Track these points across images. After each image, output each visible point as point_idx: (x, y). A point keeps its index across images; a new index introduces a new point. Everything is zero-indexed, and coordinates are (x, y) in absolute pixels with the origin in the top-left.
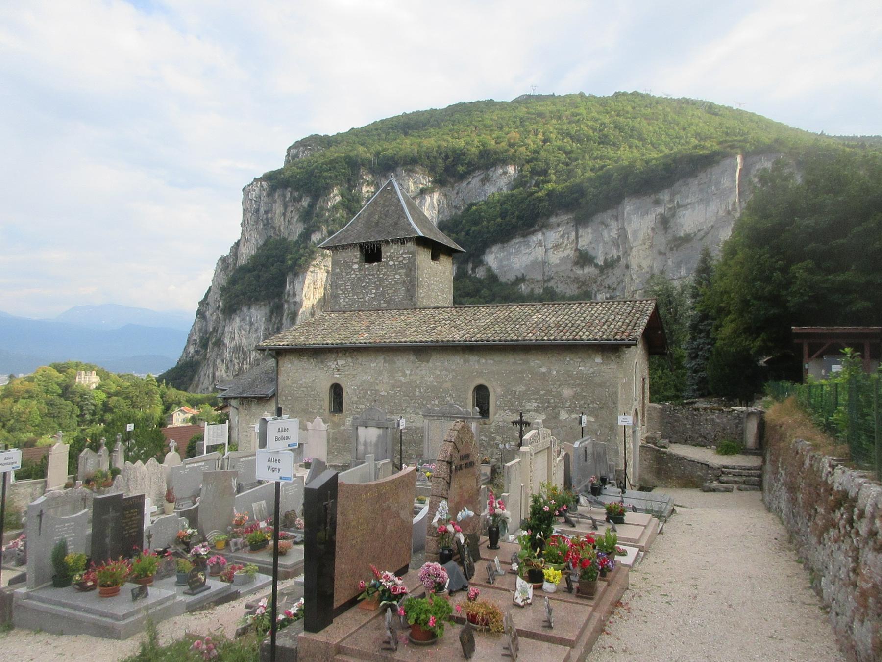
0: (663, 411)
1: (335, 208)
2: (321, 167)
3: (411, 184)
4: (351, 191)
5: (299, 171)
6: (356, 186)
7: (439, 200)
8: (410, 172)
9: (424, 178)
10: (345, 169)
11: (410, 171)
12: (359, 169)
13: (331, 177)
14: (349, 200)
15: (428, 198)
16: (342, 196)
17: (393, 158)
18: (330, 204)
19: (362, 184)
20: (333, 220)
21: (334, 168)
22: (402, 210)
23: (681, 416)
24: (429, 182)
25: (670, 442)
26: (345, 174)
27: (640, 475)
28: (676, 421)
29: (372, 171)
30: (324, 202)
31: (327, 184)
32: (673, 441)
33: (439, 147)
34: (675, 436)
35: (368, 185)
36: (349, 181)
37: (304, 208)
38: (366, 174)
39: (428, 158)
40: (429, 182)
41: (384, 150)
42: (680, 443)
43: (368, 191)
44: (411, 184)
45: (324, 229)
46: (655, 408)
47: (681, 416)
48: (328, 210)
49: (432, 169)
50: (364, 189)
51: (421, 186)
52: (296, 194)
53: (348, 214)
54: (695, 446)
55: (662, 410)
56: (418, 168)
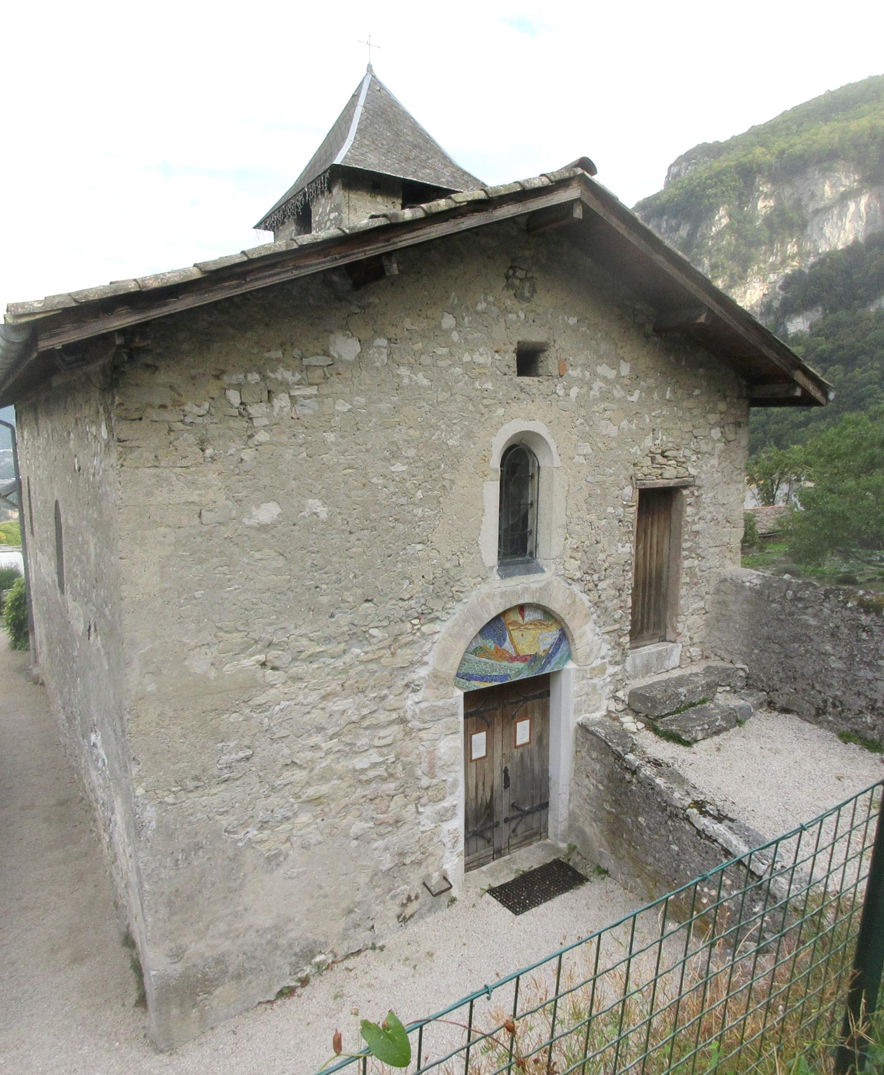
0: (760, 595)
1: (720, 234)
2: (705, 183)
3: (827, 188)
4: (742, 209)
5: (677, 192)
6: (749, 202)
7: (868, 206)
8: (827, 171)
9: (847, 177)
10: (735, 181)
11: (826, 170)
12: (755, 179)
13: (716, 195)
14: (739, 222)
15: (852, 206)
16: (730, 217)
17: (801, 157)
18: (714, 229)
19: (758, 198)
20: (718, 250)
21: (722, 182)
22: (359, 131)
23: (812, 622)
24: (855, 181)
25: (771, 705)
26: (734, 189)
27: (573, 816)
28: (796, 638)
29: (773, 179)
30: (706, 227)
31: (711, 204)
32: (781, 702)
33: (873, 128)
34: (788, 688)
35: (766, 198)
36: (741, 195)
37: (682, 238)
38: (763, 183)
39: (855, 147)
40: (855, 181)
41: (791, 146)
42: (801, 715)
43: (765, 207)
44: (827, 188)
45: (706, 262)
46: (739, 587)
47: (812, 622)
48: (712, 238)
49: (860, 163)
50: (760, 204)
51: (842, 189)
52: (673, 222)
53: (737, 240)
54: (845, 738)
55: (759, 593)
56: (839, 164)
